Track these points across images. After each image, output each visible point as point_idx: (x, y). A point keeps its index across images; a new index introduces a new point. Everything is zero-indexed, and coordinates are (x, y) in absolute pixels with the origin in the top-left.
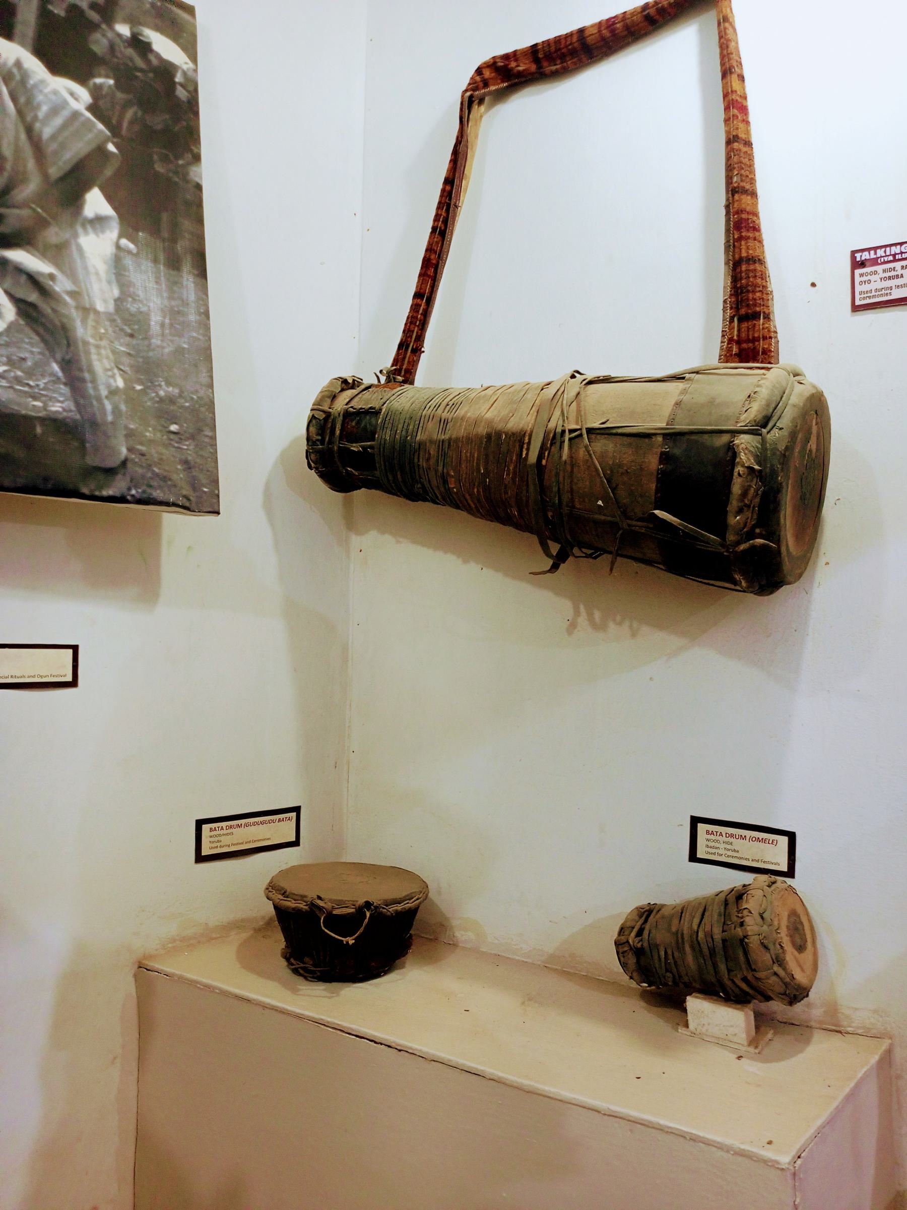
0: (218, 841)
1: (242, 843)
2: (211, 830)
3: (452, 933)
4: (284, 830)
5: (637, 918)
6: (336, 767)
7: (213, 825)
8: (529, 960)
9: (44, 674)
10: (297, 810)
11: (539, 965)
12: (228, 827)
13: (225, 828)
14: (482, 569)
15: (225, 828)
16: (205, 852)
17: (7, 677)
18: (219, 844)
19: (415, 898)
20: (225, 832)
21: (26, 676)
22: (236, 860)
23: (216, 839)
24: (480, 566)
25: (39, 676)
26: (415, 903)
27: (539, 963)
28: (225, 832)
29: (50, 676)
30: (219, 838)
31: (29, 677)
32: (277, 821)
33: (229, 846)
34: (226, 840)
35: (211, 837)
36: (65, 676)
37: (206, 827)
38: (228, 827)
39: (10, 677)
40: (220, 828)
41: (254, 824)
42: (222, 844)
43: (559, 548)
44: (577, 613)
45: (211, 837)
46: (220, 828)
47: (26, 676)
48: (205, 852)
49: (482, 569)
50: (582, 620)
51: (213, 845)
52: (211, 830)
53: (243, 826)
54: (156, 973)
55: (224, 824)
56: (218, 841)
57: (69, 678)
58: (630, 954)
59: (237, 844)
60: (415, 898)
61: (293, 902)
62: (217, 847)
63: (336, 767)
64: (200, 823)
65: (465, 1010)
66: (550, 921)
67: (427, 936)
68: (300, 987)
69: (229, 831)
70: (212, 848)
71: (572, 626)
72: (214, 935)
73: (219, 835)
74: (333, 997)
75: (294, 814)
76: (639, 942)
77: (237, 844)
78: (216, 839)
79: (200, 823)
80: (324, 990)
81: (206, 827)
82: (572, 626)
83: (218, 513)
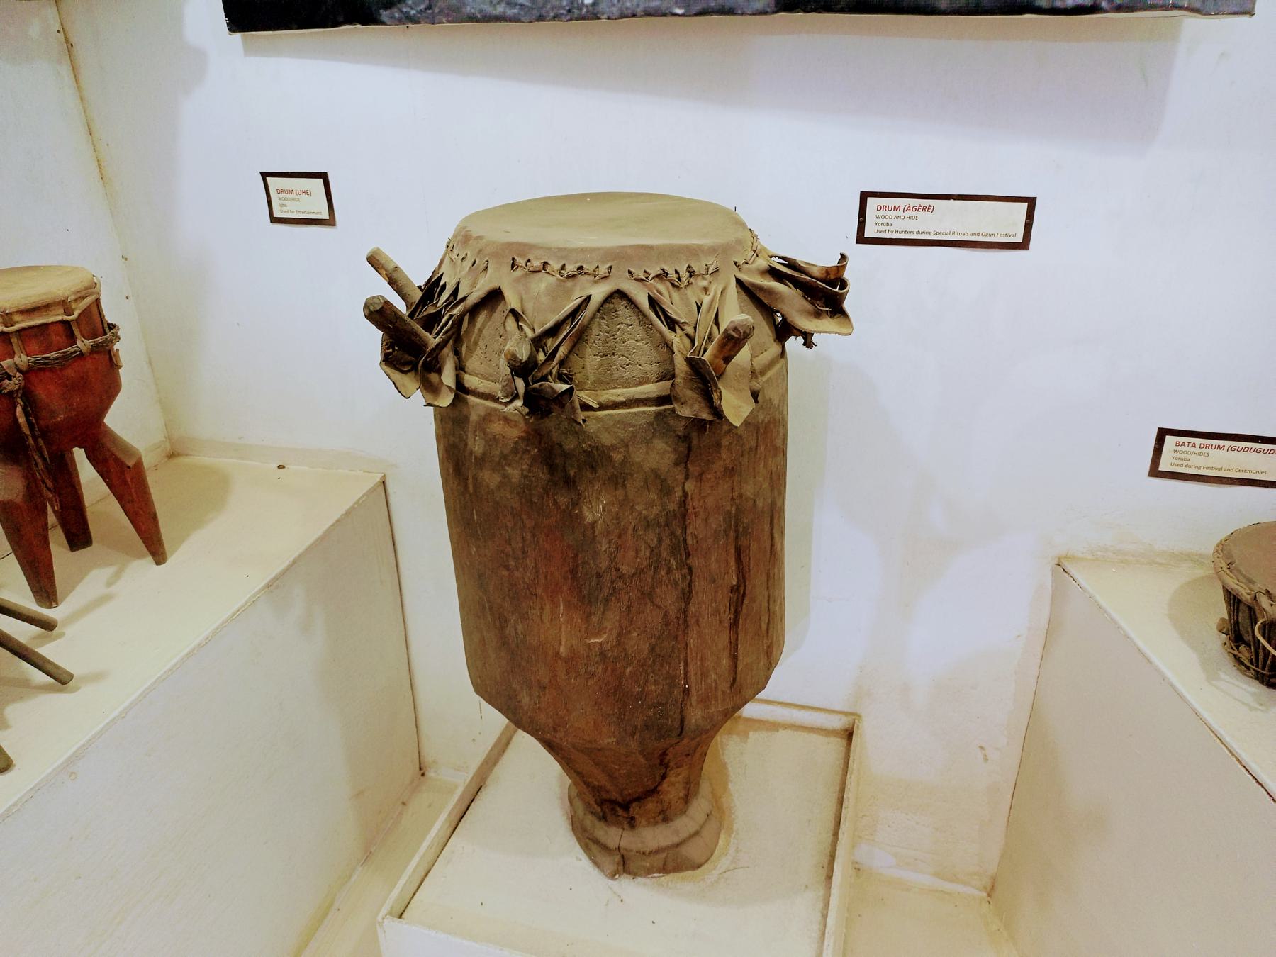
0: (1185, 459)
1: (1220, 469)
2: (1177, 444)
13: (1198, 446)
15: (1198, 446)
16: (1163, 466)
18: (1185, 463)
20: (1197, 450)
21: (970, 234)
22: (1210, 486)
23: (1183, 456)
28: (1197, 450)
30: (1187, 456)
31: (972, 235)
33: (1199, 468)
38: (1202, 446)
40: (1190, 445)
41: (1244, 450)
42: (1190, 463)
46: (1190, 445)
47: (970, 234)
48: (1163, 466)
51: (1177, 462)
52: (1177, 444)
53: (1226, 449)
55: (1198, 441)
56: (1185, 459)
57: (1019, 239)
61: (1236, 581)
62: (1182, 465)
64: (1162, 434)
68: (1222, 675)
69: (1204, 450)
72: (1158, 560)
74: (1256, 709)
77: (1212, 468)
78: (1183, 456)
79: (1162, 434)
80: (1253, 694)
83: (1250, 13)
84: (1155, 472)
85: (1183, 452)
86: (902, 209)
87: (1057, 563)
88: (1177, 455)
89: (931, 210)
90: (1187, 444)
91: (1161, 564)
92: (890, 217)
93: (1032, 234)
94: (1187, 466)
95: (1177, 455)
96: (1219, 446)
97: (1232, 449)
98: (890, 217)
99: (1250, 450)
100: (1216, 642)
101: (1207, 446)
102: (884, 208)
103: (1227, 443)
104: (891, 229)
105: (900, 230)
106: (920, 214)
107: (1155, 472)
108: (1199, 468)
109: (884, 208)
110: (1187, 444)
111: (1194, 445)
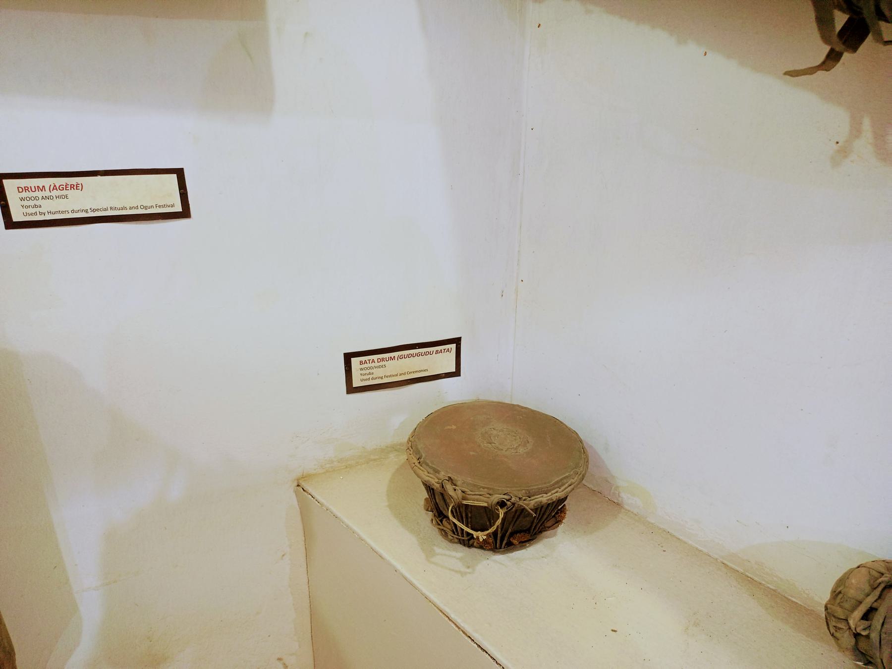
0: (370, 374)
1: (397, 375)
2: (361, 363)
3: (617, 492)
4: (444, 361)
5: (867, 589)
6: (502, 295)
7: (363, 359)
8: (705, 550)
9: (149, 205)
10: (457, 341)
11: (716, 559)
12: (379, 360)
13: (376, 361)
14: (705, 55)
15: (376, 361)
16: (356, 383)
17: (106, 210)
18: (371, 376)
19: (566, 485)
20: (376, 364)
21: (128, 208)
23: (367, 372)
24: (703, 50)
25: (142, 207)
26: (567, 490)
27: (716, 556)
28: (376, 364)
29: (155, 206)
30: (370, 371)
31: (131, 208)
32: (434, 352)
33: (382, 378)
34: (378, 372)
35: (361, 369)
36: (173, 206)
37: (355, 361)
38: (379, 360)
39: (109, 209)
40: (371, 361)
41: (408, 356)
42: (374, 376)
43: (846, 20)
44: (856, 131)
45: (361, 369)
46: (371, 361)
48: (356, 383)
49: (705, 55)
50: (864, 145)
51: (365, 377)
52: (361, 363)
53: (396, 359)
54: (310, 496)
55: (375, 357)
56: (370, 374)
58: (847, 632)
59: (391, 376)
60: (566, 485)
61: (426, 473)
63: (502, 295)
65: (613, 630)
66: (737, 521)
67: (591, 486)
68: (438, 550)
69: (381, 363)
70: (364, 380)
71: (843, 151)
72: (372, 457)
73: (371, 368)
74: (466, 573)
75: (454, 346)
76: (864, 629)
77: (391, 376)
78: (367, 372)
80: (461, 559)
81: (355, 361)
82: (843, 151)
84: (351, 389)
85: (367, 368)
86: (48, 189)
87: (296, 484)
88: (363, 372)
89: (80, 188)
90: (368, 362)
91: (375, 460)
92: (36, 198)
93: (190, 203)
94: (373, 379)
95: (363, 372)
96: (391, 357)
97: (400, 357)
98: (36, 198)
99: (412, 355)
100: (426, 518)
101: (383, 360)
102: (26, 189)
103: (396, 354)
104: (41, 210)
105: (53, 210)
106: (70, 193)
107: (351, 389)
108: (382, 378)
109: (26, 189)
110: (368, 362)
111: (373, 361)
